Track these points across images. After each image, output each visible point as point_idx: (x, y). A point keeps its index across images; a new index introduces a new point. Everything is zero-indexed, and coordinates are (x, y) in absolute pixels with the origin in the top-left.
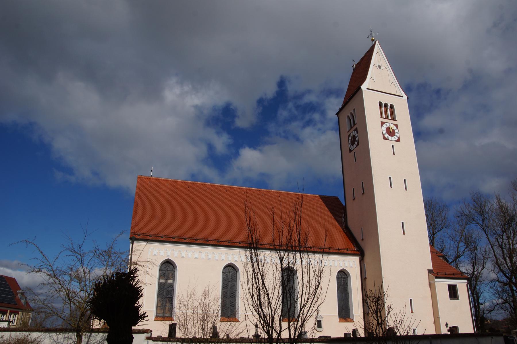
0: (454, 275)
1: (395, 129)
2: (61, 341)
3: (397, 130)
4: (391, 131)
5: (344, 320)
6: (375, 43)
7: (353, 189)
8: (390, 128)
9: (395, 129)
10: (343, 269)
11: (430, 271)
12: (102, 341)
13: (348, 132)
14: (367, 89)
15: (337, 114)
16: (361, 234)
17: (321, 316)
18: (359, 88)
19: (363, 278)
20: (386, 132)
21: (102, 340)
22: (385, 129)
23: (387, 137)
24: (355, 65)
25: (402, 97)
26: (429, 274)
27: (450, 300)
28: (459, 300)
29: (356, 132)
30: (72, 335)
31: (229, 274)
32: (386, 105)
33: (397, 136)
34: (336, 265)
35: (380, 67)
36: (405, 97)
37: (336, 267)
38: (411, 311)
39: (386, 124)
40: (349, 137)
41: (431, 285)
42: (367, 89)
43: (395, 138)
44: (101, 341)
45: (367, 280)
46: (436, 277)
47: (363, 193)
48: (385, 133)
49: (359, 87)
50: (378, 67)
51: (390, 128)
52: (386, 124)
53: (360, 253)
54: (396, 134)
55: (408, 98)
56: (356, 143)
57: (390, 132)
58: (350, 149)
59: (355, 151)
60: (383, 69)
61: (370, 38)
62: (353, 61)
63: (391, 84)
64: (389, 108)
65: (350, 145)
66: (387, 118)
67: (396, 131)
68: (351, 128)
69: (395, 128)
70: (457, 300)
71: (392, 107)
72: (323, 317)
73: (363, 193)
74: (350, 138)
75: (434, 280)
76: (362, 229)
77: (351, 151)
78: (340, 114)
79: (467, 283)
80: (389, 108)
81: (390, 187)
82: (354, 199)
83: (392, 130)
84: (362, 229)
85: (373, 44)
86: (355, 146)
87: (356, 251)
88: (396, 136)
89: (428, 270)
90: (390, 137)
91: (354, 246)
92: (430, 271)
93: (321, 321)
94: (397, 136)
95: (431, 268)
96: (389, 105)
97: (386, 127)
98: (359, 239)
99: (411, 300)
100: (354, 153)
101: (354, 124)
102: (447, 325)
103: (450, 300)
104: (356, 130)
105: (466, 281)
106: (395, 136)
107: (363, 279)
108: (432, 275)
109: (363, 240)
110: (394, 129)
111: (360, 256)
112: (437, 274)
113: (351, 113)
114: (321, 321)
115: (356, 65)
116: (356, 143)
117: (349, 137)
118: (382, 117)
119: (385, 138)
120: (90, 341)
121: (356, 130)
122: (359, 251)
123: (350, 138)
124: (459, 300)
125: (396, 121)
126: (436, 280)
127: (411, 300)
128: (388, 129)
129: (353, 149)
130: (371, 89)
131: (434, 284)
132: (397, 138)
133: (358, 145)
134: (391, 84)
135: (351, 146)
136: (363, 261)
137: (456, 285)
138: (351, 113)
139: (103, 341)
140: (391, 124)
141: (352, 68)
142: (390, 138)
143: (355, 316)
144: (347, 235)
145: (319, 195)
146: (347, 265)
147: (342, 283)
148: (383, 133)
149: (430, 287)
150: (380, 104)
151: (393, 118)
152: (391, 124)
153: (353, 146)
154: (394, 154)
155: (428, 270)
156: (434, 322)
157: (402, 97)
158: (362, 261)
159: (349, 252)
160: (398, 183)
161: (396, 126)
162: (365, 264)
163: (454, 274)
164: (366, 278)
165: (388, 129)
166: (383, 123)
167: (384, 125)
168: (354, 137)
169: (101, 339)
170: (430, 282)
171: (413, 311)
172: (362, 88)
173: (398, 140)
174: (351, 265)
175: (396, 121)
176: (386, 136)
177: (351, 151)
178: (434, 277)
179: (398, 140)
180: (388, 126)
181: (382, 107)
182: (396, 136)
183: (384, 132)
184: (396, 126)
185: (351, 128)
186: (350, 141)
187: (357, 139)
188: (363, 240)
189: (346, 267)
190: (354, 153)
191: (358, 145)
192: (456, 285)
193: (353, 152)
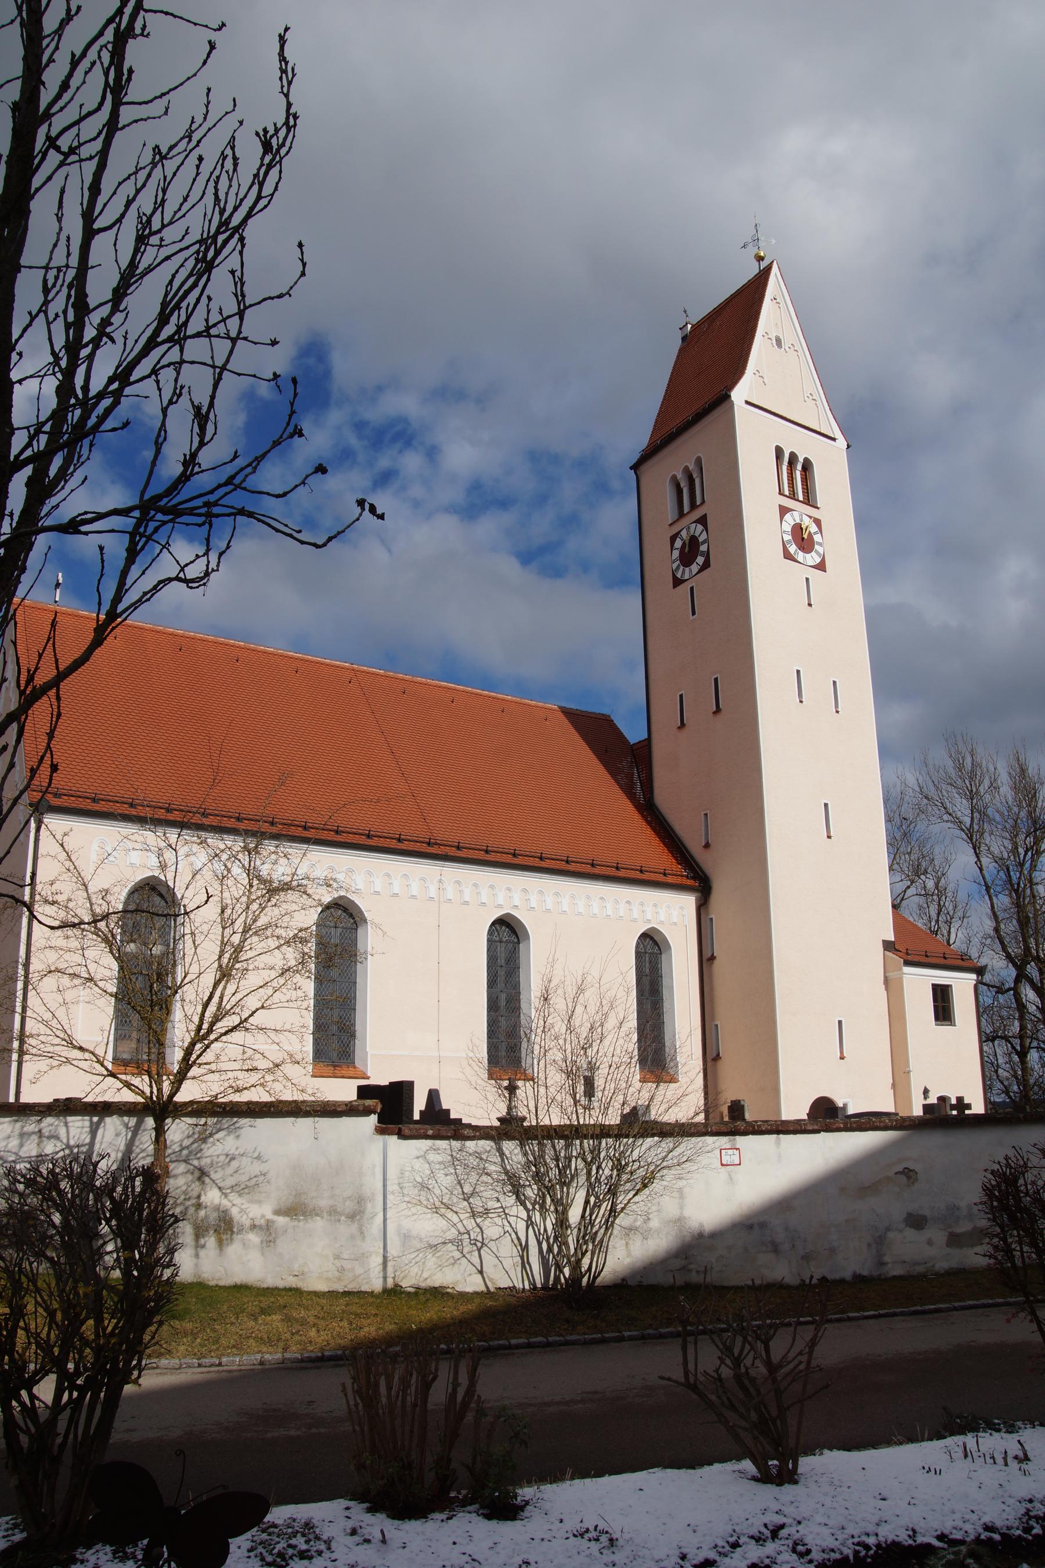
0: (945, 958)
1: (816, 533)
2: (10, 1145)
3: (819, 535)
4: (805, 536)
6: (769, 269)
7: (681, 696)
9: (816, 533)
10: (653, 929)
11: (888, 946)
12: (192, 1143)
13: (671, 525)
14: (747, 403)
15: (635, 467)
16: (703, 828)
18: (724, 398)
19: (707, 954)
20: (790, 537)
21: (191, 1140)
22: (789, 529)
23: (795, 553)
24: (689, 326)
25: (834, 439)
26: (887, 952)
27: (936, 1025)
28: (955, 1025)
29: (700, 527)
30: (57, 1126)
31: (333, 930)
32: (793, 457)
34: (635, 916)
36: (841, 443)
37: (635, 920)
39: (792, 516)
40: (673, 539)
41: (891, 985)
42: (747, 403)
43: (813, 558)
44: (186, 1143)
45: (716, 962)
46: (907, 963)
47: (718, 711)
48: (789, 541)
49: (726, 393)
51: (802, 529)
52: (792, 516)
53: (700, 886)
54: (816, 547)
55: (848, 447)
56: (700, 560)
57: (803, 538)
58: (674, 577)
59: (694, 584)
60: (787, 349)
61: (752, 251)
62: (685, 311)
63: (806, 399)
65: (675, 566)
66: (793, 496)
67: (817, 538)
68: (681, 515)
69: (814, 528)
70: (951, 1025)
71: (807, 466)
73: (718, 711)
74: (678, 543)
75: (901, 969)
76: (706, 815)
77: (677, 582)
78: (644, 468)
79: (975, 982)
80: (799, 467)
81: (798, 700)
82: (683, 725)
84: (706, 815)
85: (760, 271)
86: (695, 568)
87: (687, 877)
88: (817, 552)
89: (883, 941)
90: (801, 553)
91: (679, 864)
92: (888, 946)
96: (801, 459)
97: (793, 523)
98: (694, 845)
100: (692, 589)
101: (693, 506)
102: (926, 1092)
103: (936, 1025)
104: (703, 521)
105: (974, 976)
106: (813, 553)
107: (706, 960)
108: (894, 956)
109: (707, 846)
110: (812, 532)
111: (699, 894)
112: (907, 954)
113: (686, 470)
115: (693, 326)
116: (700, 560)
117: (673, 539)
118: (781, 493)
119: (788, 556)
120: (137, 1143)
121: (703, 521)
122: (694, 878)
123: (678, 543)
124: (955, 1025)
125: (818, 508)
126: (907, 969)
127: (840, 1022)
128: (798, 530)
129: (686, 577)
131: (900, 981)
132: (818, 560)
133: (706, 565)
134: (806, 399)
135: (682, 567)
136: (707, 909)
137: (950, 986)
138: (686, 470)
139: (196, 1145)
141: (679, 335)
142: (800, 556)
144: (653, 829)
145: (560, 707)
147: (648, 970)
148: (785, 539)
149: (887, 989)
150: (779, 452)
151: (809, 499)
152: (804, 516)
153: (687, 569)
154: (810, 605)
155: (883, 941)
156: (894, 1086)
157: (834, 439)
158: (702, 907)
159: (670, 879)
160: (817, 689)
161: (818, 522)
162: (713, 916)
163: (947, 956)
164: (712, 958)
165: (798, 530)
166: (784, 511)
167: (788, 517)
168: (694, 541)
169: (188, 1137)
170: (887, 975)
171: (845, 1055)
172: (733, 399)
173: (821, 566)
175: (818, 508)
176: (793, 549)
177: (677, 582)
178: (902, 960)
179: (821, 566)
180: (798, 521)
181: (782, 464)
182: (817, 552)
183: (788, 537)
184: (818, 522)
185: (681, 515)
186: (676, 554)
187: (703, 548)
188: (707, 846)
189: (662, 923)
190: (692, 589)
191: (706, 565)
192: (950, 986)
193: (685, 588)
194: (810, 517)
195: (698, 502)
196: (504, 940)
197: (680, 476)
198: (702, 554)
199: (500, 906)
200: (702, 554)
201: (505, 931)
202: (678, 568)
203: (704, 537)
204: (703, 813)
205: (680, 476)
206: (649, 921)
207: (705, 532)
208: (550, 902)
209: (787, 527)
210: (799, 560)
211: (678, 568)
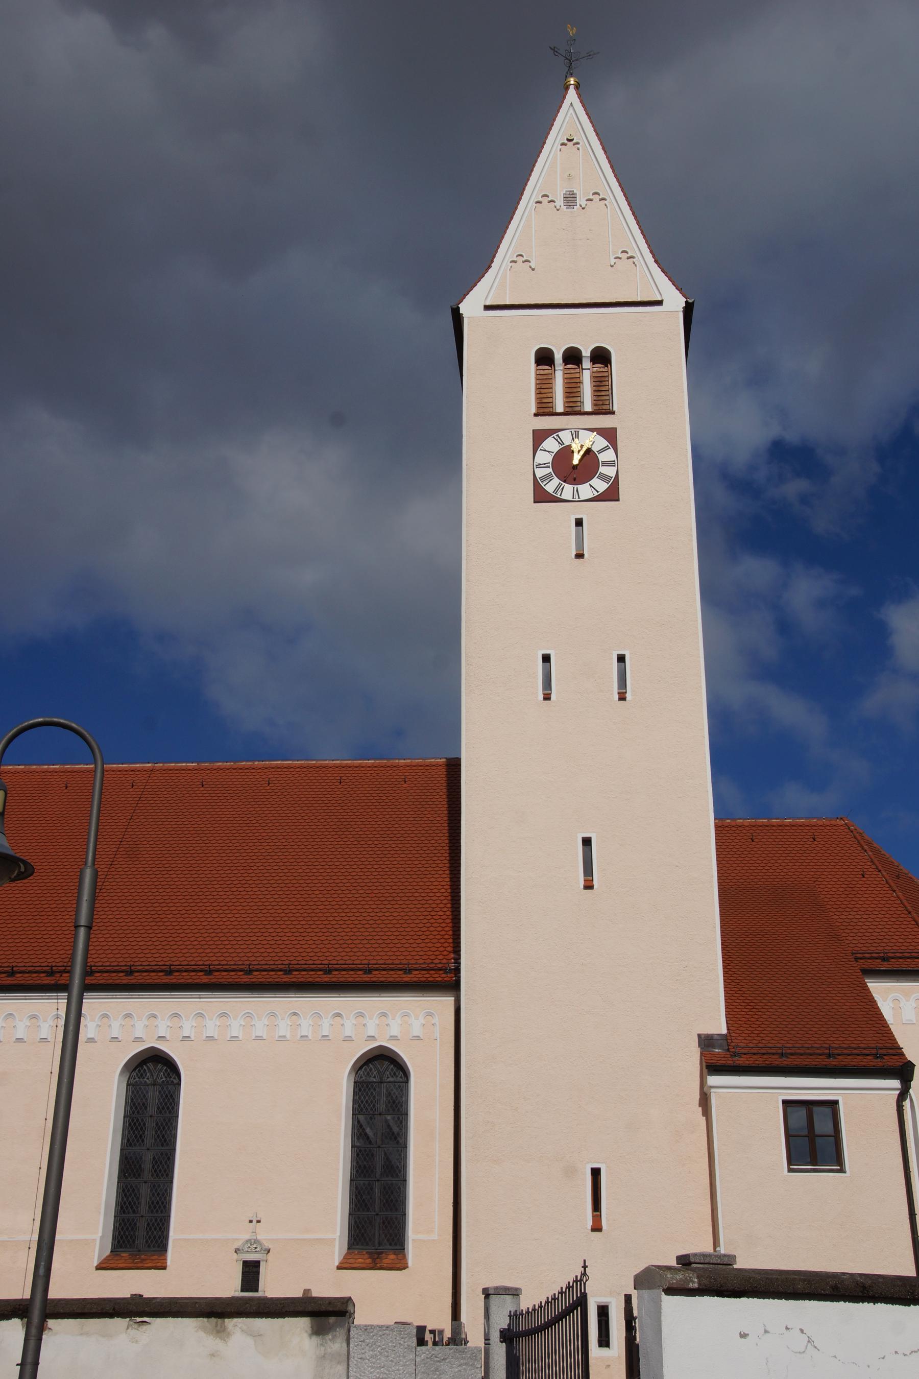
5: (369, 1261)
8: (575, 447)
11: (706, 1042)
14: (487, 308)
17: (261, 1244)
20: (550, 470)
27: (790, 1170)
33: (604, 478)
34: (348, 1031)
35: (570, 199)
37: (348, 1039)
38: (590, 1223)
42: (487, 308)
48: (548, 477)
50: (560, 202)
64: (586, 364)
69: (598, 442)
71: (601, 357)
72: (267, 1245)
83: (582, 453)
89: (699, 1035)
92: (706, 1042)
93: (256, 1264)
94: (604, 478)
95: (719, 1026)
96: (586, 353)
99: (596, 1173)
103: (790, 1170)
105: (896, 1083)
110: (595, 449)
114: (256, 1264)
118: (544, 409)
127: (596, 1173)
130: (508, 303)
132: (602, 486)
140: (581, 432)
142: (568, 491)
143: (413, 1240)
146: (395, 1030)
148: (538, 476)
150: (544, 358)
152: (581, 432)
155: (699, 1035)
161: (610, 435)
166: (539, 437)
174: (416, 1030)
179: (611, 494)
189: (394, 1038)
194: (592, 430)
196: (159, 1081)
199: (138, 1040)
201: (161, 1070)
206: (372, 1038)
208: (211, 1027)
209: (544, 457)
210: (563, 497)
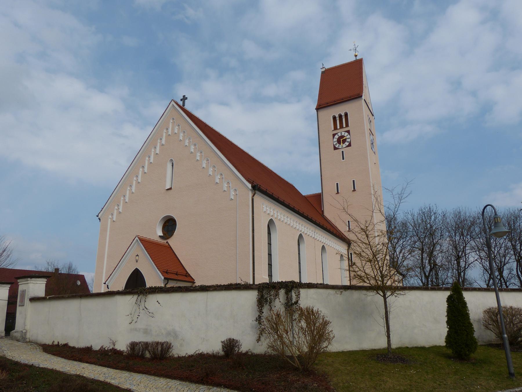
29: (347, 134)
40: (334, 135)
65: (335, 143)
74: (336, 137)
77: (335, 148)
86: (344, 146)
100: (343, 152)
101: (341, 127)
116: (347, 144)
117: (334, 135)
121: (348, 132)
123: (336, 137)
177: (335, 148)
185: (335, 128)
186: (335, 140)
190: (343, 152)
191: (350, 145)
195: (344, 126)
197: (337, 116)
198: (348, 142)
200: (348, 142)
202: (336, 144)
203: (349, 136)
204: (347, 221)
205: (337, 116)
207: (349, 135)
211: (336, 144)
